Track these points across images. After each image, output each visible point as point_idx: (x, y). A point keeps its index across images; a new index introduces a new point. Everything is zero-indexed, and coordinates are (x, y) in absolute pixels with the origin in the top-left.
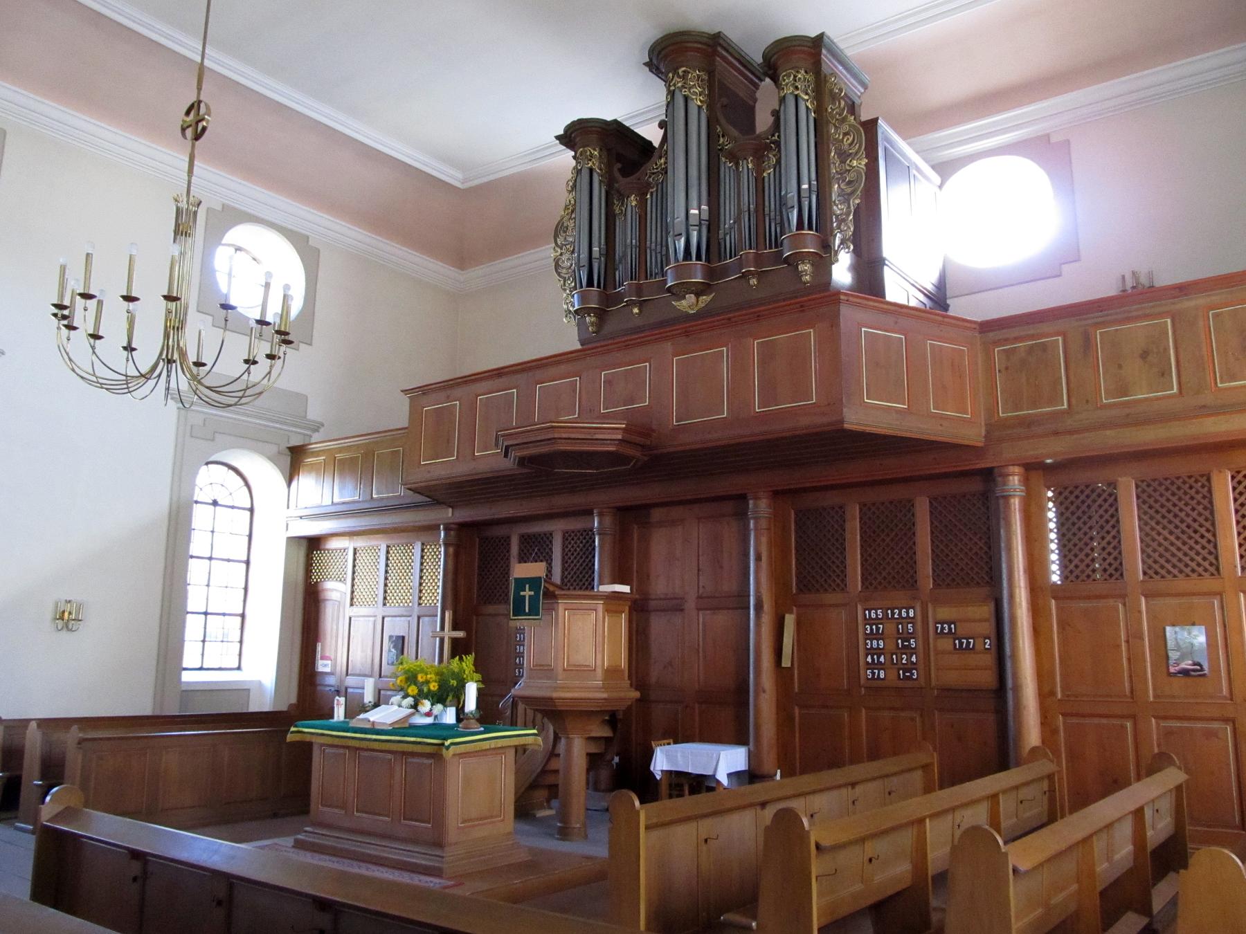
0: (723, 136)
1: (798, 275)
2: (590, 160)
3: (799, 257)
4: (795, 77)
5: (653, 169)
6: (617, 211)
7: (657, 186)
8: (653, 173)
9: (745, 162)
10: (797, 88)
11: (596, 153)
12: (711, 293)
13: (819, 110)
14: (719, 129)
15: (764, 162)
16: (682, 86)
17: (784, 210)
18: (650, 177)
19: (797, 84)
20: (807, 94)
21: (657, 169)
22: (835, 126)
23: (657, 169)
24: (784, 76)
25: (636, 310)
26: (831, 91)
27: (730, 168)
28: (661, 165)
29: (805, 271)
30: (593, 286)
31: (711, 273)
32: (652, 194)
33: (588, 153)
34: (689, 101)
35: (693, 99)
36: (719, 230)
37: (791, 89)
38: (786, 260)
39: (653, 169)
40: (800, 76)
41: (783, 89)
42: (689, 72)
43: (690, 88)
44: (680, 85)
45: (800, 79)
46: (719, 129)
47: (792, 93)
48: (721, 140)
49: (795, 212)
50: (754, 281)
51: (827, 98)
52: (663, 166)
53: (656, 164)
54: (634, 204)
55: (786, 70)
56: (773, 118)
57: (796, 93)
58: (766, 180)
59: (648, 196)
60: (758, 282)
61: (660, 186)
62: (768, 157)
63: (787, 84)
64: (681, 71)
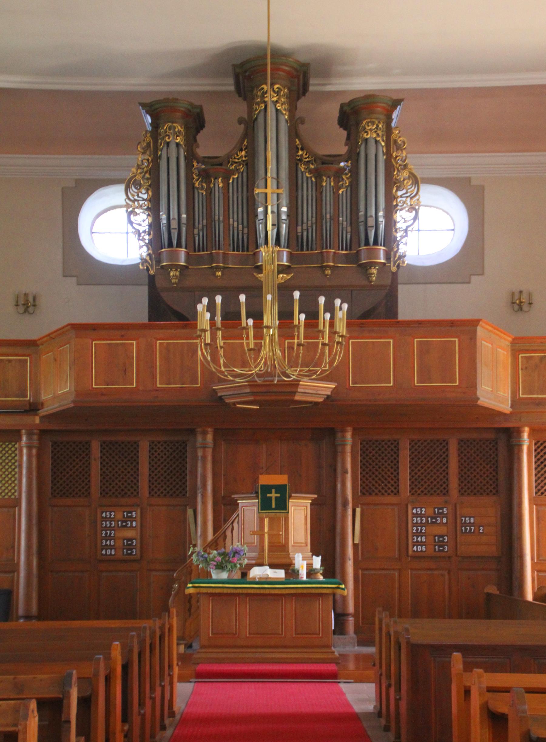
0: (302, 149)
1: (368, 276)
2: (179, 136)
3: (374, 264)
4: (377, 126)
5: (235, 158)
6: (197, 185)
7: (238, 174)
8: (236, 163)
9: (328, 179)
10: (378, 135)
11: (182, 130)
12: (288, 273)
13: (388, 154)
14: (298, 142)
15: (339, 182)
16: (277, 101)
17: (362, 228)
18: (232, 165)
19: (379, 132)
20: (383, 141)
21: (238, 159)
22: (398, 170)
23: (238, 159)
24: (369, 122)
25: (219, 274)
26: (395, 142)
27: (307, 178)
28: (242, 157)
29: (374, 274)
30: (181, 247)
31: (291, 257)
32: (233, 179)
33: (177, 130)
34: (280, 114)
35: (283, 114)
36: (297, 225)
37: (374, 135)
38: (361, 265)
39: (235, 158)
40: (380, 126)
41: (367, 132)
42: (282, 90)
43: (282, 104)
44: (275, 99)
45: (380, 128)
46: (298, 142)
47: (375, 139)
48: (300, 153)
49: (373, 231)
50: (328, 272)
51: (393, 147)
52: (244, 159)
53: (238, 156)
54: (221, 185)
55: (371, 119)
56: (347, 148)
57: (378, 139)
58: (340, 197)
59: (231, 181)
60: (332, 272)
61: (240, 175)
62: (343, 179)
63: (371, 130)
64: (276, 86)
